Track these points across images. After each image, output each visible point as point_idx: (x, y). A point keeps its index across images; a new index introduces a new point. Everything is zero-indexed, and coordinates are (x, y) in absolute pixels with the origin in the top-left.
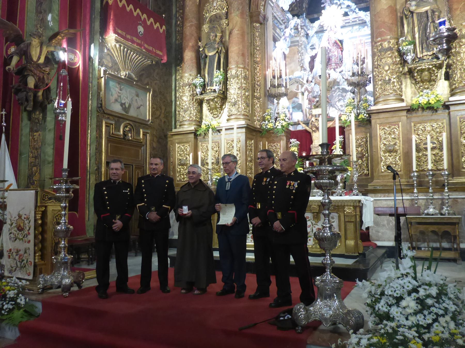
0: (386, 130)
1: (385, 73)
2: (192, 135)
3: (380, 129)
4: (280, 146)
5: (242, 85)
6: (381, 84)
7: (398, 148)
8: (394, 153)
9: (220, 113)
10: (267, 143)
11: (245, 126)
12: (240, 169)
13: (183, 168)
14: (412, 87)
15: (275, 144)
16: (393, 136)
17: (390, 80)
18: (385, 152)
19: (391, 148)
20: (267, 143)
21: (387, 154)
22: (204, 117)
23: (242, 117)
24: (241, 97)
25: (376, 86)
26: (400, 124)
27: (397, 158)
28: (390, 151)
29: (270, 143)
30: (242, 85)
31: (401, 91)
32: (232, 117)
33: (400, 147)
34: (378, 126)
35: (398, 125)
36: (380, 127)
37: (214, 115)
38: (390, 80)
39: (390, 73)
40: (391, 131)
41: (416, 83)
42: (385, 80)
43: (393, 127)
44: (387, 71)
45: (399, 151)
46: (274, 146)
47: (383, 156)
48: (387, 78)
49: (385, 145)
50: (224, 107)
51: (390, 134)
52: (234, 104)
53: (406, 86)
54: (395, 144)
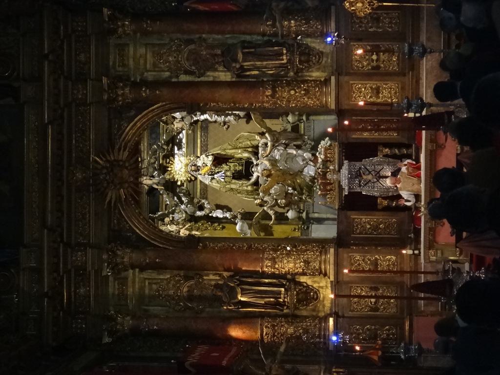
0: (356, 95)
1: (297, 94)
2: (341, 320)
3: (354, 101)
4: (358, 219)
5: (284, 254)
6: (308, 98)
7: (375, 86)
8: (379, 89)
9: (313, 290)
10: (352, 235)
11: (336, 246)
12: (386, 257)
13: (381, 335)
14: (312, 71)
15: (355, 225)
16: (363, 89)
17: (305, 90)
18: (378, 98)
19: (375, 91)
20: (352, 235)
21: (380, 95)
22: (314, 314)
23: (323, 257)
24: (299, 255)
25: (309, 104)
26: (351, 82)
27: (385, 86)
28: (378, 93)
29: (353, 231)
30: (284, 254)
31: (317, 81)
32: (323, 267)
33: (374, 84)
34: (351, 102)
35: (352, 84)
36: (352, 101)
37: (313, 297)
38: (305, 90)
39: (297, 89)
40: (358, 91)
41: (310, 67)
42: (305, 95)
43: (354, 88)
44: (296, 92)
45: (378, 85)
46: (357, 226)
47: (382, 99)
48: (303, 92)
49: (371, 97)
50: (305, 285)
51: (360, 92)
52: (307, 262)
53: (310, 76)
54: (371, 88)
